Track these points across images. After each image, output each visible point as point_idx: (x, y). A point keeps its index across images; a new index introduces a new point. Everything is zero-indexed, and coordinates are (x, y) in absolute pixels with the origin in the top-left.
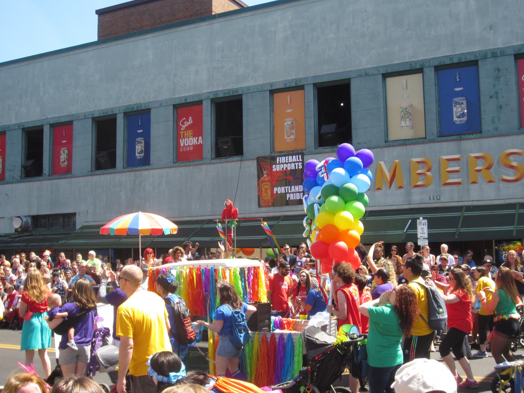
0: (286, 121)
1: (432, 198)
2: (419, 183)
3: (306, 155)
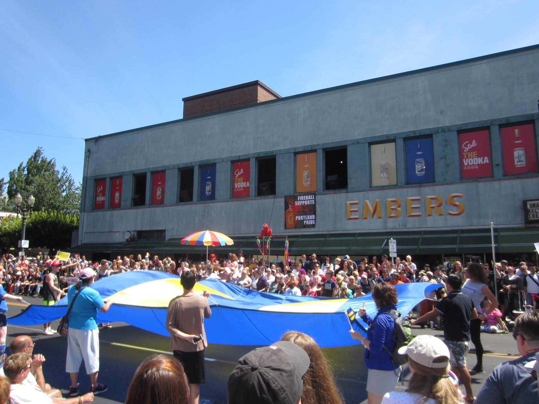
1: (401, 225)
2: (393, 215)
3: (317, 195)
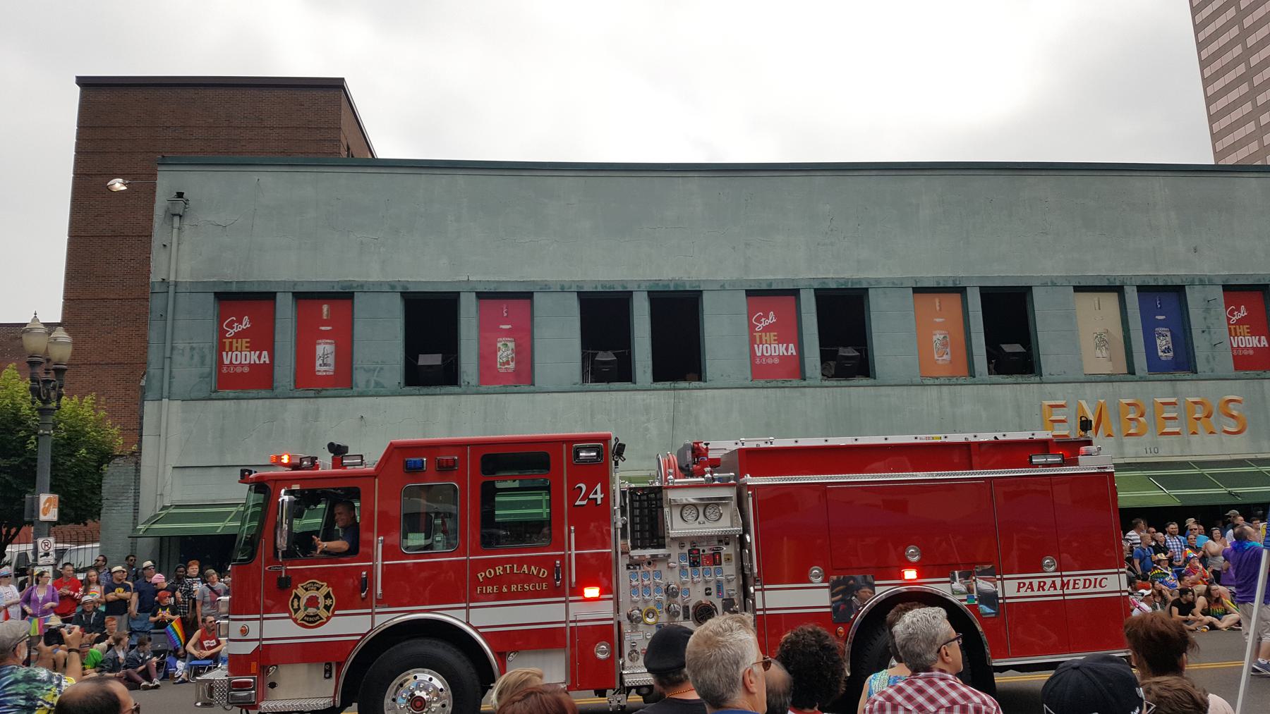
0: (935, 335)
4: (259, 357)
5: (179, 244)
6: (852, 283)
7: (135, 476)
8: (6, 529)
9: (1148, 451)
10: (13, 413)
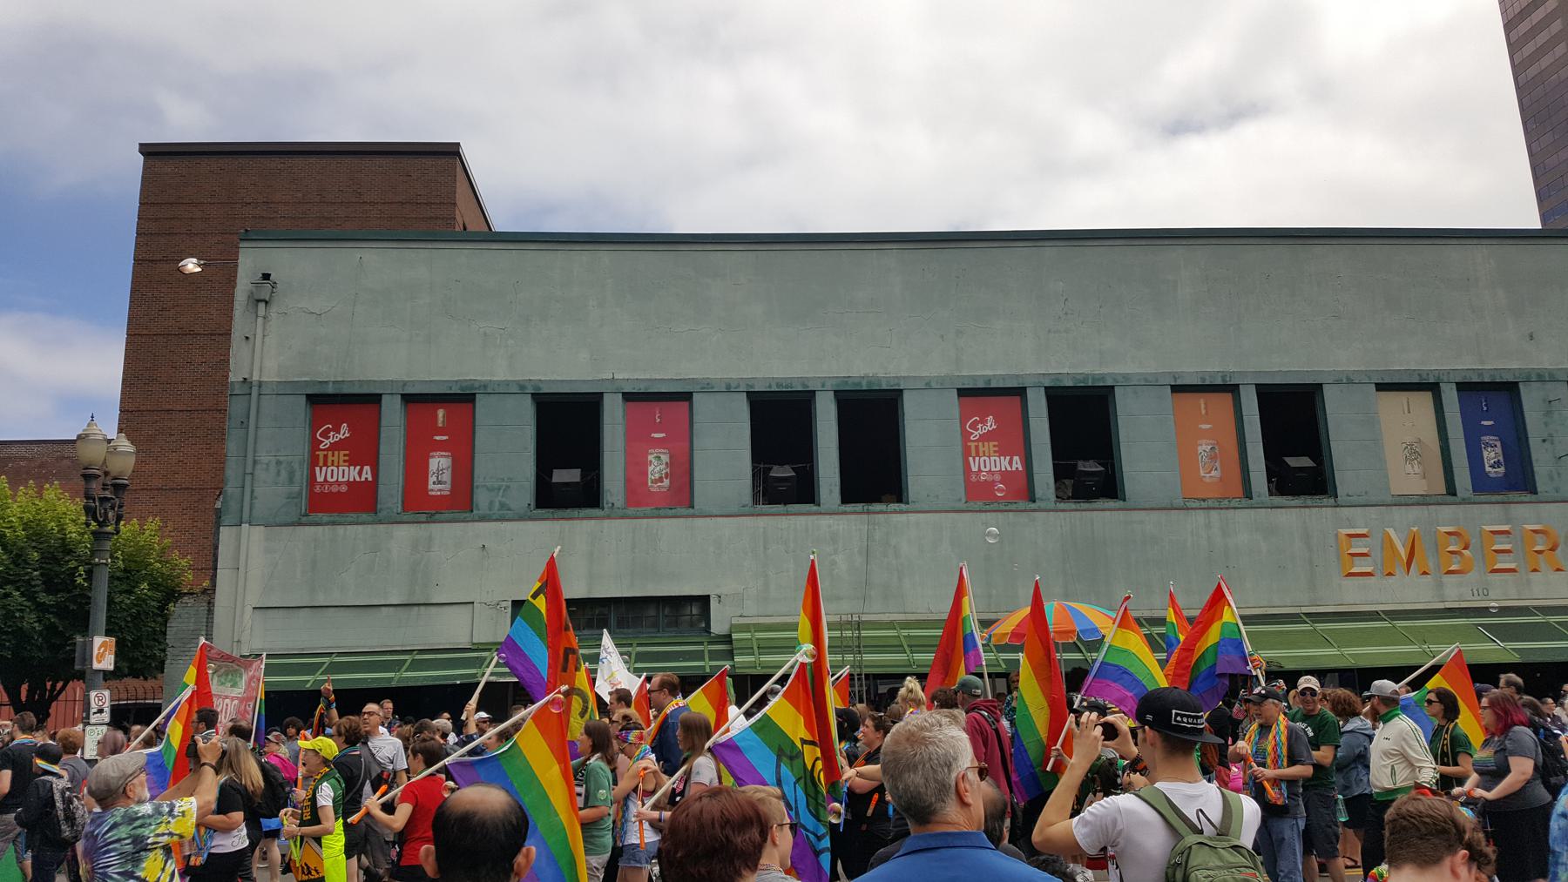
4: (360, 474)
5: (264, 336)
6: (1093, 379)
7: (207, 618)
8: (50, 683)
9: (1476, 592)
10: (60, 539)
